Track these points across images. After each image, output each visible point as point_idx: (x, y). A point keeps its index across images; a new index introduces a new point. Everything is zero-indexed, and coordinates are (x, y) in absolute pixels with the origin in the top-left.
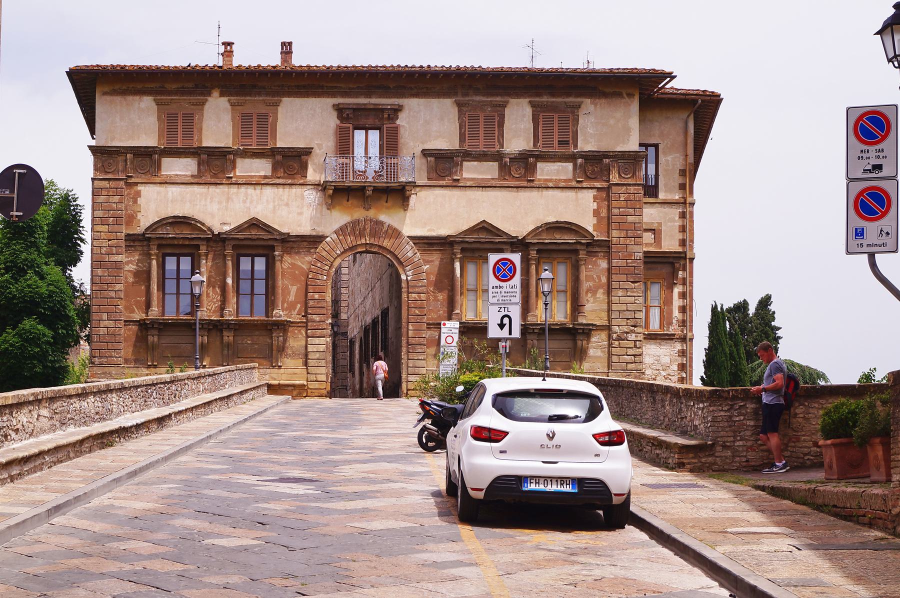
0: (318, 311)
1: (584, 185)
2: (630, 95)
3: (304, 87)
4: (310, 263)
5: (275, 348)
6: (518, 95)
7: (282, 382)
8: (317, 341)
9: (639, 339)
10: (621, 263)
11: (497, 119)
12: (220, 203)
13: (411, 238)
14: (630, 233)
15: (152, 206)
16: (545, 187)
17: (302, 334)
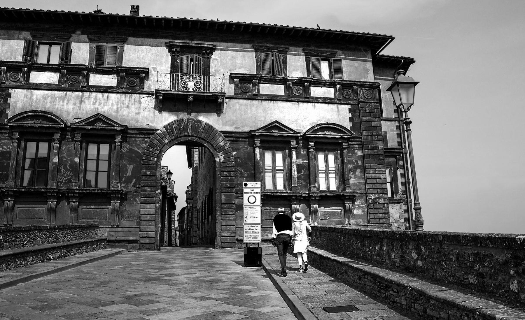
2: (366, 51)
4: (143, 148)
7: (118, 238)
8: (148, 206)
9: (386, 202)
12: (75, 104)
13: (223, 132)
15: (20, 105)
16: (317, 100)
17: (136, 201)
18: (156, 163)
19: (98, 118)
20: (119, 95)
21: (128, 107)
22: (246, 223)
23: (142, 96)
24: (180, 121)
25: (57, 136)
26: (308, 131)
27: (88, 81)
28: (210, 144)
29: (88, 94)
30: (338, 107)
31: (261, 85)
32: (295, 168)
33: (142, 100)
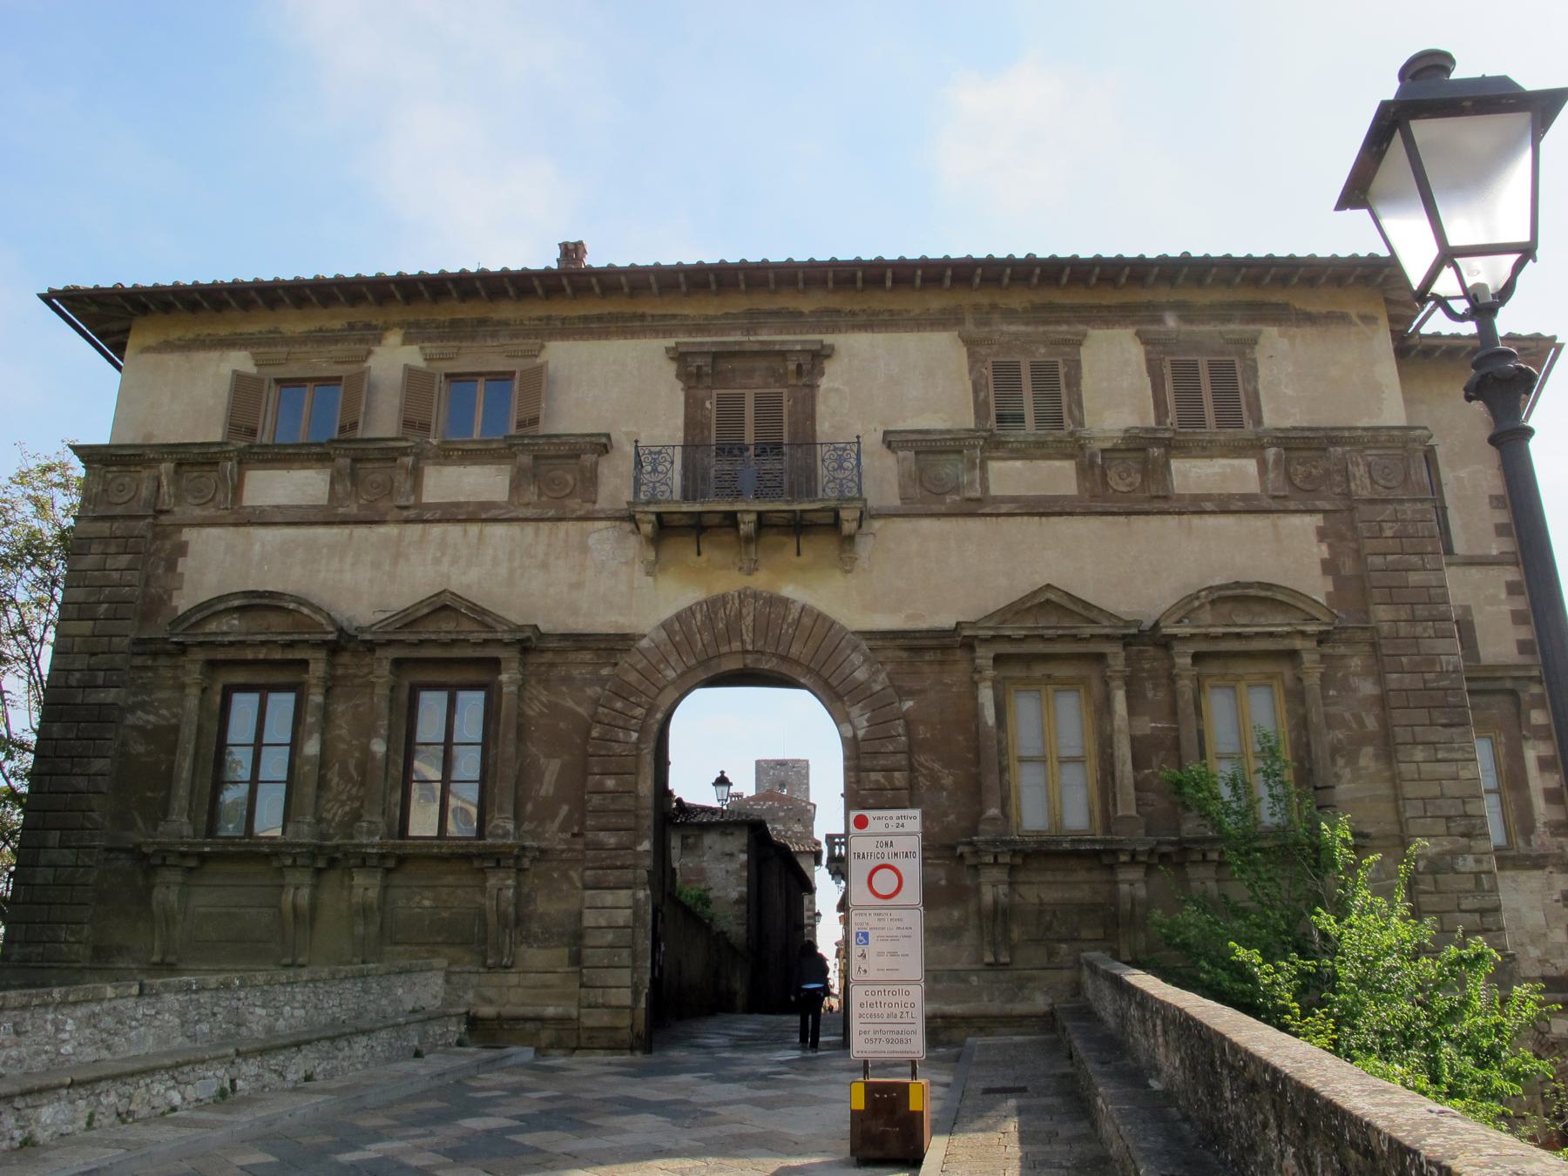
0: (613, 821)
1: (1292, 505)
2: (1367, 319)
3: (600, 318)
4: (596, 702)
5: (492, 919)
6: (1108, 323)
7: (509, 1010)
8: (609, 898)
9: (1485, 867)
10: (1409, 681)
11: (1062, 371)
14: (1421, 611)
16: (1197, 506)
17: (570, 880)
18: (638, 748)
19: (444, 606)
20: (514, 529)
21: (544, 566)
22: (863, 977)
23: (589, 525)
24: (714, 605)
25: (318, 669)
26: (1167, 614)
27: (417, 486)
28: (818, 674)
29: (417, 529)
30: (1275, 526)
31: (994, 466)
32: (1123, 751)
33: (591, 541)
